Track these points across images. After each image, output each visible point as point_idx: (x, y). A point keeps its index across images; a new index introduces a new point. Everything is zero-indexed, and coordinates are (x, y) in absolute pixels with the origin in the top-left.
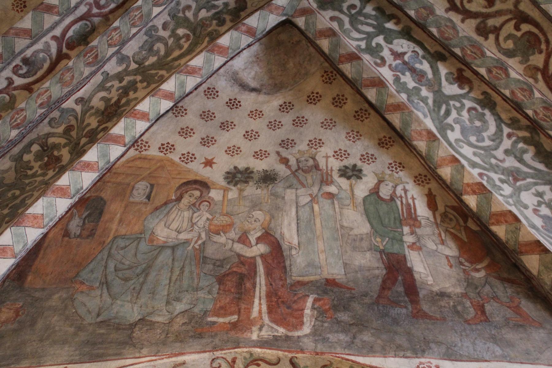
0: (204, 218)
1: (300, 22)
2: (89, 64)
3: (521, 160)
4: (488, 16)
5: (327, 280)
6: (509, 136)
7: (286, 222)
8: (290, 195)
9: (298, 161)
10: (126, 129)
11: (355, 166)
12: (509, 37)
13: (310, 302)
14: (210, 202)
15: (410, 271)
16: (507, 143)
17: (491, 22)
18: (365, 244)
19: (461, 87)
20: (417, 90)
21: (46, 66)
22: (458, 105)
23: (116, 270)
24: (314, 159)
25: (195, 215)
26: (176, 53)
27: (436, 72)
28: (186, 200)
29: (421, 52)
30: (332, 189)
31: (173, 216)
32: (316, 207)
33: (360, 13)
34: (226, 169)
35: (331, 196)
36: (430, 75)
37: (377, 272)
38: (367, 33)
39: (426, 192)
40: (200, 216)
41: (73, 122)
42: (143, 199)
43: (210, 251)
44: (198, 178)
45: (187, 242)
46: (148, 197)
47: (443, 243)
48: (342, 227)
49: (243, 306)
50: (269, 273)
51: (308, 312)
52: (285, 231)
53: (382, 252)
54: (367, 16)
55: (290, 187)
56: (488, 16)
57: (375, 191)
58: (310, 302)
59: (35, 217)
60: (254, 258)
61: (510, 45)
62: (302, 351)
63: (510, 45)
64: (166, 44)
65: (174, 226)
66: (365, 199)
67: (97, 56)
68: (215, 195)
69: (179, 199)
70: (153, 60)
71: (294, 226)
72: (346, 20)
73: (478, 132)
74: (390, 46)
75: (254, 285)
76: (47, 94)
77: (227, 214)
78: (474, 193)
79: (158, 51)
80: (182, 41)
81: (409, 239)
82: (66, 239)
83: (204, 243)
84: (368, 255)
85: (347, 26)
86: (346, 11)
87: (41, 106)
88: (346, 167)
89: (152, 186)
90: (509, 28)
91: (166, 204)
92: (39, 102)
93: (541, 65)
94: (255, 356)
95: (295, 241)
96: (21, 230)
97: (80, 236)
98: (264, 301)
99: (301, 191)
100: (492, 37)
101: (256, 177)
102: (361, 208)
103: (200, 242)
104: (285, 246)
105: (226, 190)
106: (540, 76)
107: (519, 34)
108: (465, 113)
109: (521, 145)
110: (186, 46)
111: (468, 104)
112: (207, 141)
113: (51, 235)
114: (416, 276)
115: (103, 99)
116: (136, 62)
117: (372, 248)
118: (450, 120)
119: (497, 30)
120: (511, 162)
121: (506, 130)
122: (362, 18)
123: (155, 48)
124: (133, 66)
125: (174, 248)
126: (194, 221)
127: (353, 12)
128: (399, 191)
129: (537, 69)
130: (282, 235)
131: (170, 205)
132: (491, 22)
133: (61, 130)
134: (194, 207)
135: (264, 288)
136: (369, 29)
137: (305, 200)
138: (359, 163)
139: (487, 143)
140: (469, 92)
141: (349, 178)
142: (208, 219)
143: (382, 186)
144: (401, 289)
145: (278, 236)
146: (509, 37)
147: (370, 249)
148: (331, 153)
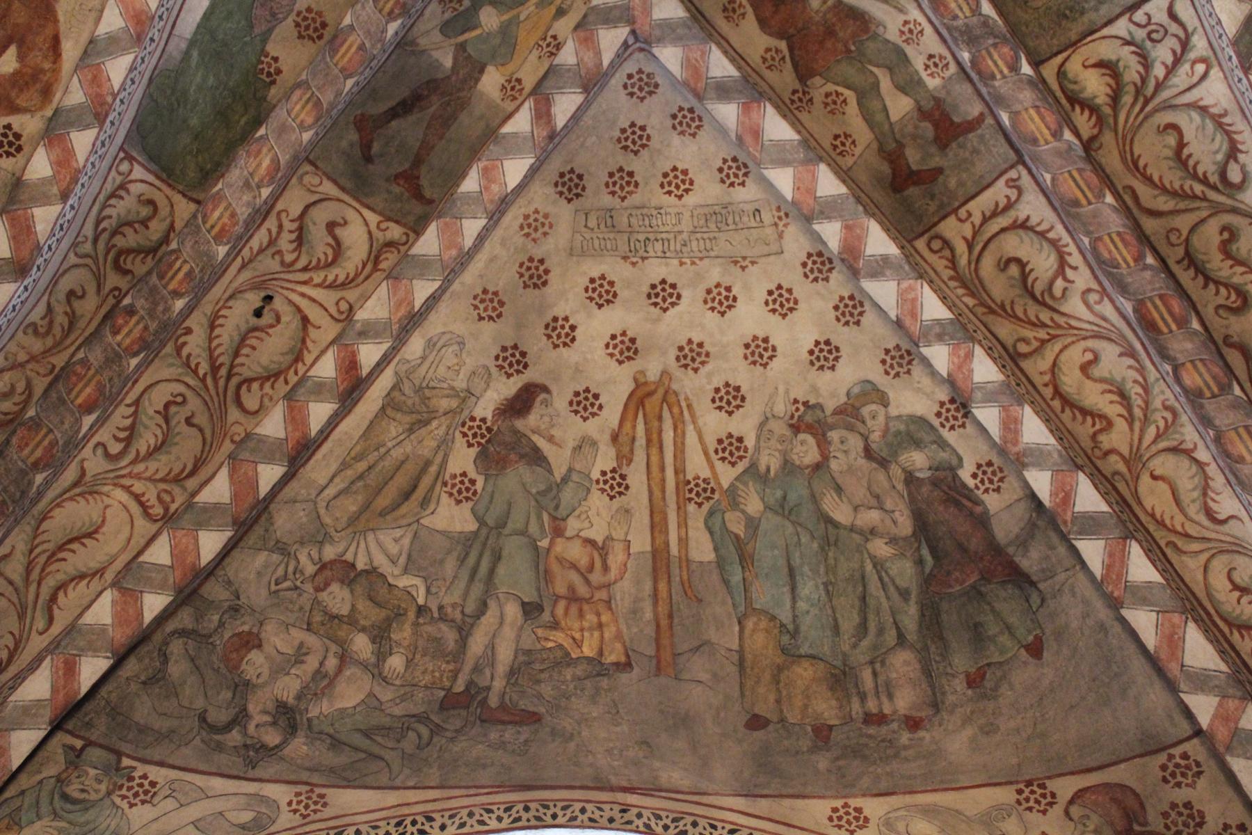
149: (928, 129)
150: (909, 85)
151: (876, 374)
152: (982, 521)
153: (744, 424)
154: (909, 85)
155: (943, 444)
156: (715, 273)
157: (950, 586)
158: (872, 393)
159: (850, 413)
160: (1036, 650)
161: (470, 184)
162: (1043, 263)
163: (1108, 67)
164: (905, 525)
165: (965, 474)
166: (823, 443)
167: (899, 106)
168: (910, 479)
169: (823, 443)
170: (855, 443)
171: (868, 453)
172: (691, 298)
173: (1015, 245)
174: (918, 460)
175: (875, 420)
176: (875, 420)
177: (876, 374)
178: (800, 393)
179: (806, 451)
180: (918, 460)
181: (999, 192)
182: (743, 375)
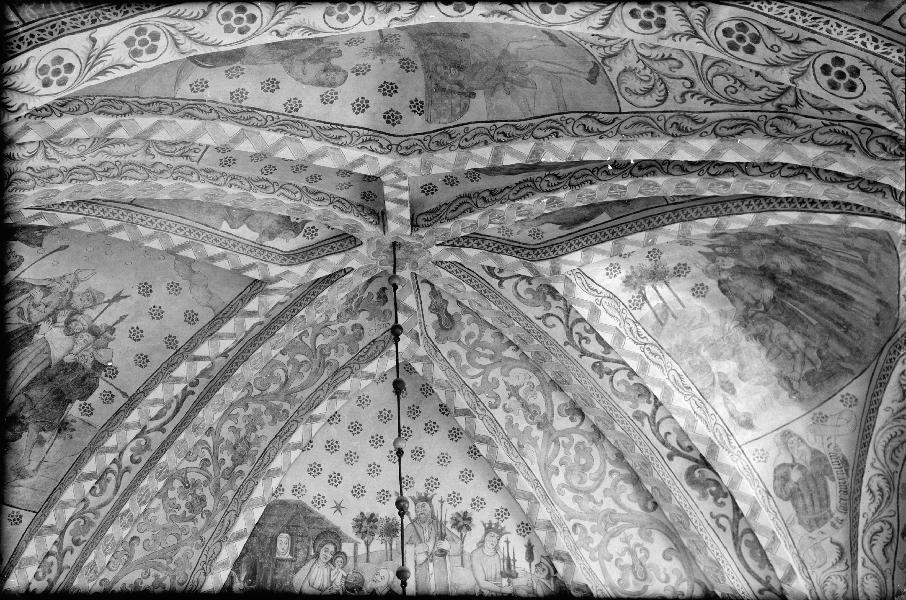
0: (340, 576)
1: (418, 367)
4: (605, 360)
16: (608, 482)
19: (572, 419)
20: (527, 430)
21: (174, 406)
22: (566, 440)
25: (333, 572)
27: (550, 404)
29: (535, 381)
30: (445, 545)
33: (478, 343)
35: (443, 553)
38: (485, 367)
39: (526, 542)
41: (207, 455)
61: (622, 389)
64: (286, 372)
70: (274, 388)
72: (462, 352)
73: (585, 468)
74: (506, 379)
85: (465, 362)
86: (463, 340)
100: (606, 378)
101: (381, 525)
106: (646, 421)
107: (632, 383)
108: (572, 451)
109: (621, 483)
111: (577, 438)
112: (335, 479)
118: (556, 463)
120: (609, 504)
121: (610, 467)
122: (479, 349)
126: (332, 579)
127: (472, 341)
133: (197, 463)
136: (487, 362)
137: (422, 558)
138: (469, 510)
139: (589, 483)
140: (580, 424)
142: (343, 576)
148: (445, 498)
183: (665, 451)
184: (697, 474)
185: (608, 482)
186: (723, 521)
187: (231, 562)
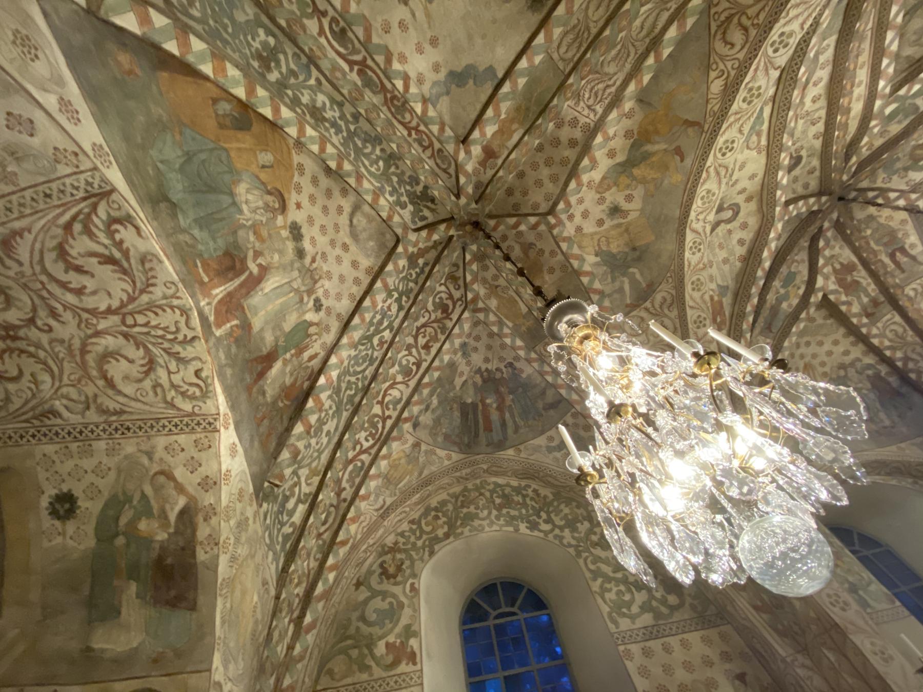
2: (350, 93)
3: (346, 390)
4: (417, 347)
5: (250, 324)
6: (358, 379)
7: (277, 279)
8: (296, 274)
9: (316, 269)
10: (311, 137)
11: (322, 305)
12: (407, 360)
13: (235, 322)
14: (275, 218)
15: (270, 367)
17: (414, 350)
18: (278, 333)
23: (204, 161)
24: (320, 278)
26: (367, 163)
28: (269, 198)
31: (256, 192)
32: (292, 294)
33: (409, 280)
34: (298, 221)
35: (302, 300)
36: (382, 328)
37: (264, 349)
40: (262, 215)
42: (261, 163)
43: (241, 233)
44: (287, 202)
45: (241, 212)
46: (263, 167)
47: (291, 375)
48: (284, 315)
49: (216, 281)
50: (241, 285)
51: (228, 325)
52: (271, 281)
53: (276, 345)
54: (407, 285)
55: (300, 271)
56: (417, 347)
57: (311, 324)
58: (235, 322)
59: (224, 70)
60: (248, 268)
61: (404, 362)
62: (207, 341)
63: (404, 362)
64: (371, 153)
65: (250, 197)
66: (305, 321)
67: (357, 100)
68: (280, 220)
69: (269, 193)
71: (276, 285)
72: (404, 274)
75: (232, 280)
76: (322, 57)
77: (270, 235)
78: (327, 380)
79: (366, 147)
80: (375, 166)
81: (288, 356)
82: (211, 102)
83: (245, 225)
84: (273, 338)
87: (311, 50)
88: (320, 301)
89: (272, 167)
90: (412, 360)
91: (263, 183)
92: (314, 48)
93: (397, 380)
94: (189, 313)
95: (266, 291)
96: (209, 58)
97: (217, 115)
98: (224, 293)
99: (299, 280)
100: (407, 353)
102: (299, 321)
103: (245, 222)
104: (262, 285)
105: (284, 227)
110: (373, 170)
113: (208, 84)
114: (269, 373)
115: (324, 104)
116: (355, 129)
117: (277, 339)
119: (410, 354)
123: (368, 145)
124: (352, 128)
125: (234, 204)
126: (258, 211)
128: (314, 337)
129: (395, 379)
130: (268, 280)
131: (263, 187)
132: (414, 350)
133: (293, 66)
134: (267, 207)
135: (232, 288)
138: (324, 307)
139: (351, 370)
141: (315, 305)
143: (315, 327)
144: (259, 369)
145: (267, 277)
146: (408, 361)
147: (276, 338)
149: (872, 304)
150: (868, 295)
151: (860, 356)
152: (889, 383)
153: (827, 369)
154: (868, 295)
155: (876, 369)
156: (819, 338)
157: (826, 391)
158: (859, 360)
159: (852, 364)
160: (911, 409)
161: (794, 329)
162: (900, 330)
163: (914, 289)
164: (869, 386)
165: (883, 374)
166: (846, 371)
167: (865, 300)
168: (868, 376)
169: (846, 371)
170: (853, 370)
171: (857, 372)
172: (813, 344)
173: (893, 327)
174: (870, 372)
175: (859, 365)
176: (859, 365)
177: (860, 356)
178: (840, 361)
179: (842, 373)
180: (870, 372)
181: (889, 316)
182: (826, 359)
183: (380, 398)
184: (376, 419)
185: (353, 379)
186: (358, 447)
187: (253, 100)
